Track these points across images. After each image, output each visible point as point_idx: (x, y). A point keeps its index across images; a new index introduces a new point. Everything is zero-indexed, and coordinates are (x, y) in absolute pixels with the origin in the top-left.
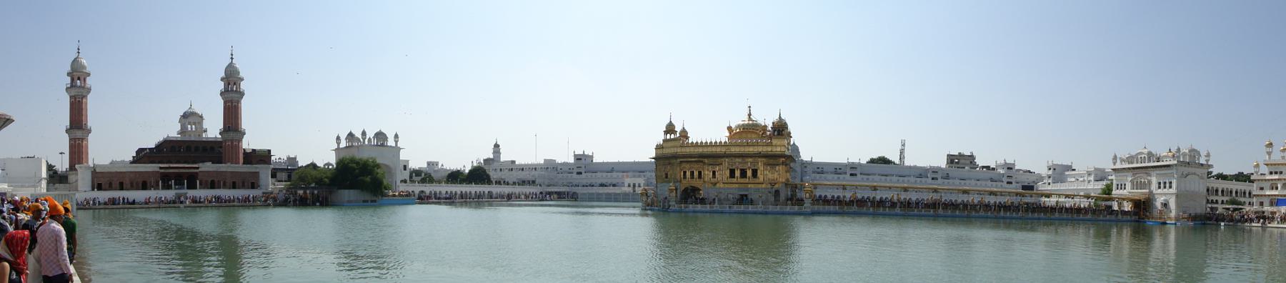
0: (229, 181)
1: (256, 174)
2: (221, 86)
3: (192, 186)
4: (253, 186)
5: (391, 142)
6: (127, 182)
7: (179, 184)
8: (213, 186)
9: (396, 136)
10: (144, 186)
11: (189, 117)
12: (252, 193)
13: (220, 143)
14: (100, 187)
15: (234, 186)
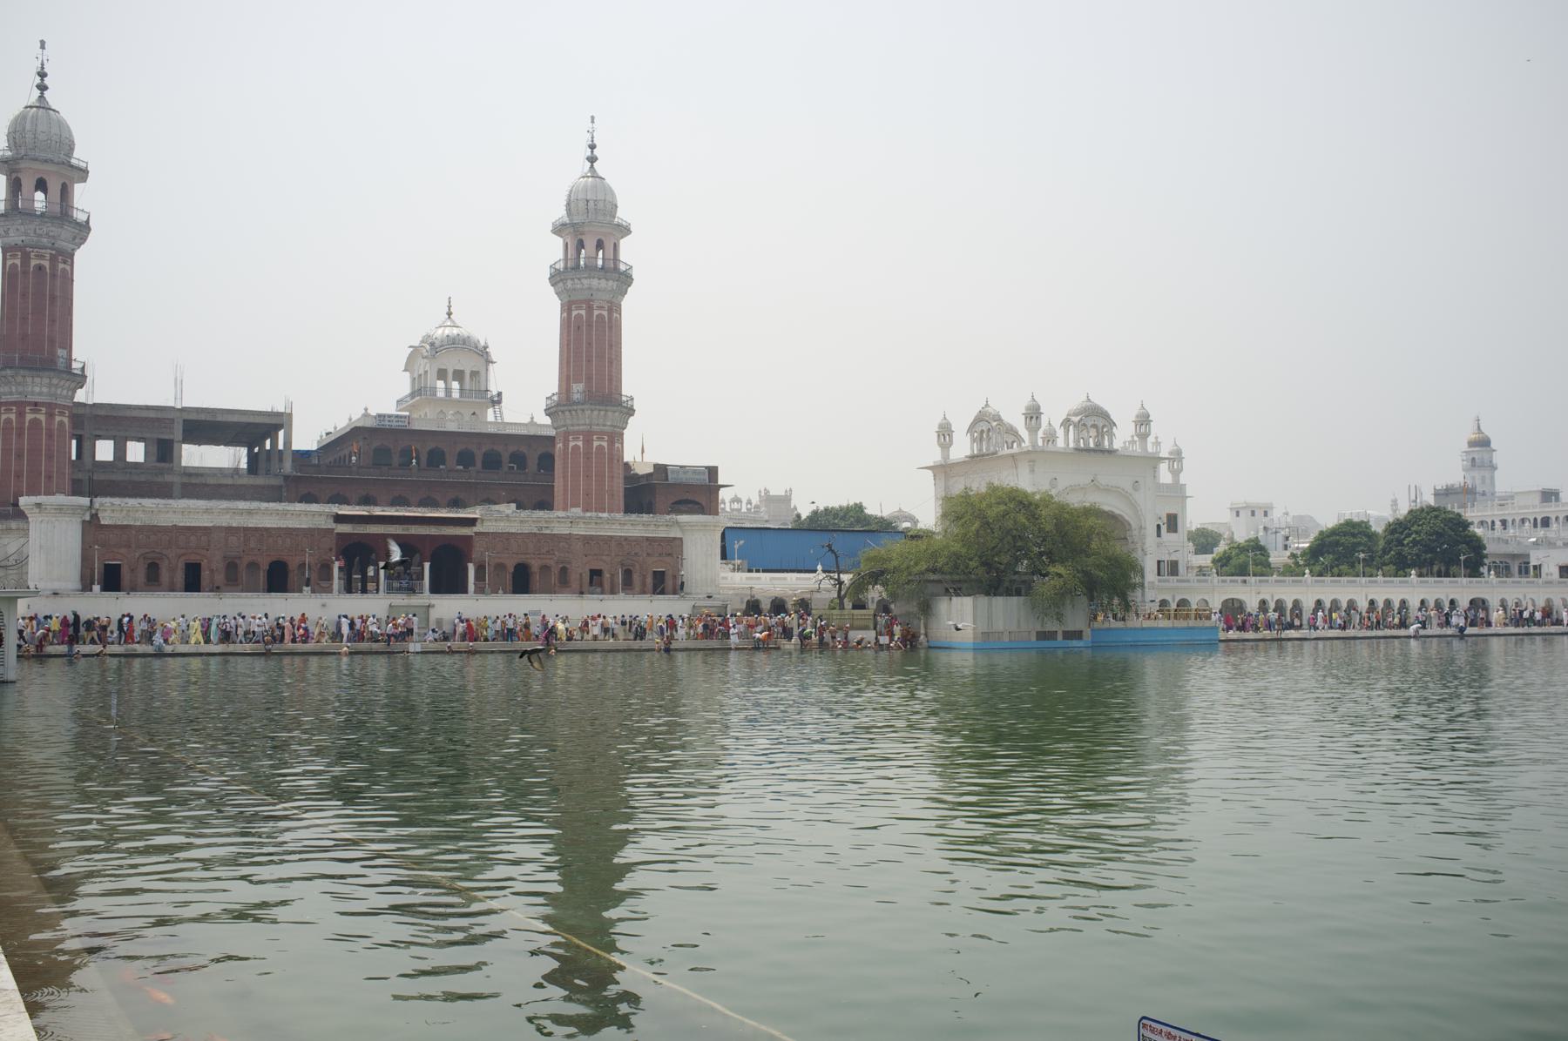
0: (580, 569)
1: (672, 548)
2: (554, 250)
3: (449, 582)
4: (663, 583)
5: (1122, 436)
6: (213, 566)
7: (403, 578)
8: (522, 582)
9: (1143, 420)
10: (278, 579)
11: (456, 359)
12: (649, 608)
13: (551, 439)
14: (112, 581)
15: (595, 581)
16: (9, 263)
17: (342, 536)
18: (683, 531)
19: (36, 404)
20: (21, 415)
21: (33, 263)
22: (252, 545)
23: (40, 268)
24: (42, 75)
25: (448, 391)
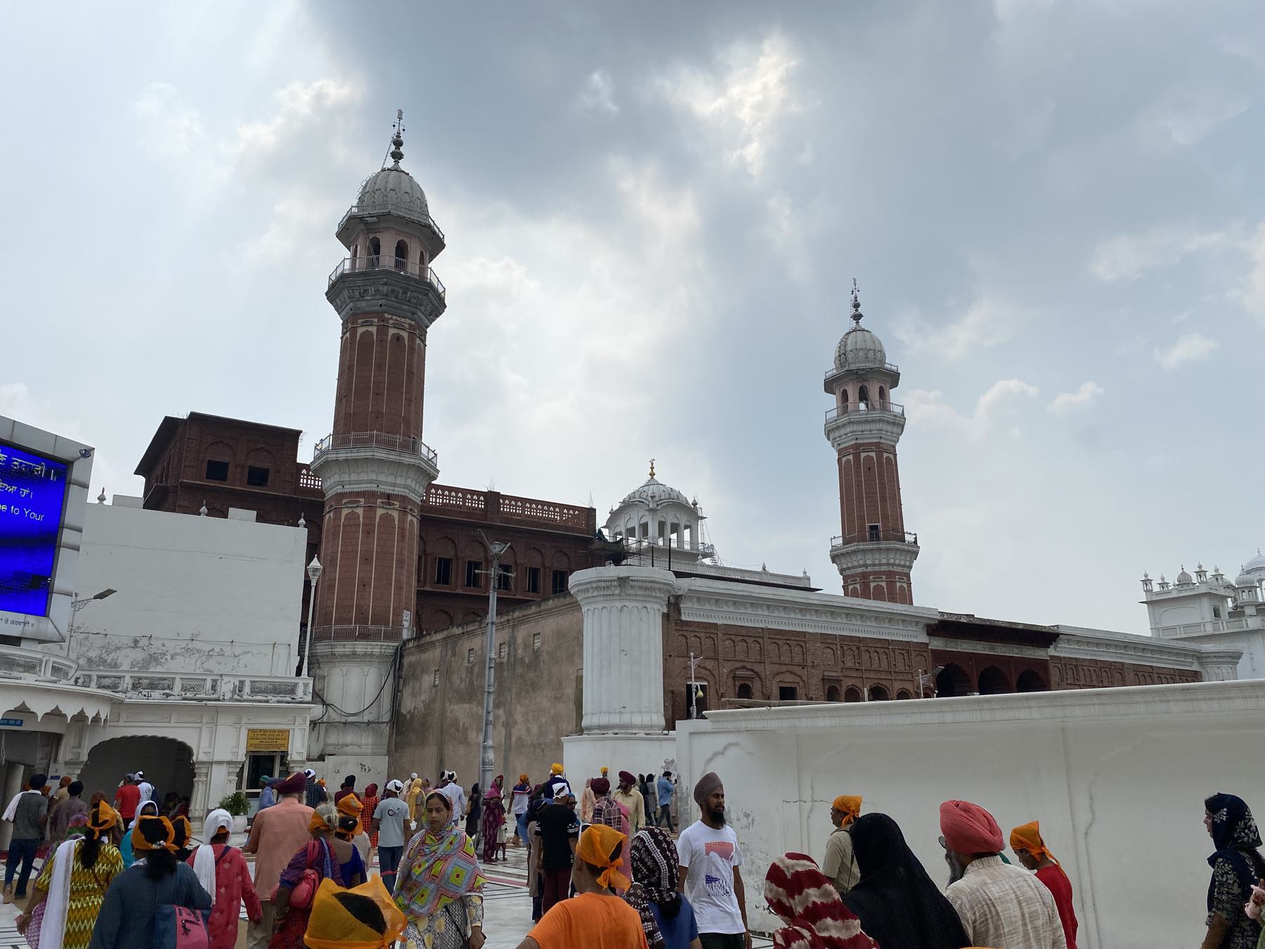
16: (360, 330)
17: (938, 655)
18: (1201, 664)
19: (389, 496)
20: (370, 509)
21: (392, 331)
22: (849, 664)
23: (398, 338)
24: (398, 143)
25: (680, 540)
